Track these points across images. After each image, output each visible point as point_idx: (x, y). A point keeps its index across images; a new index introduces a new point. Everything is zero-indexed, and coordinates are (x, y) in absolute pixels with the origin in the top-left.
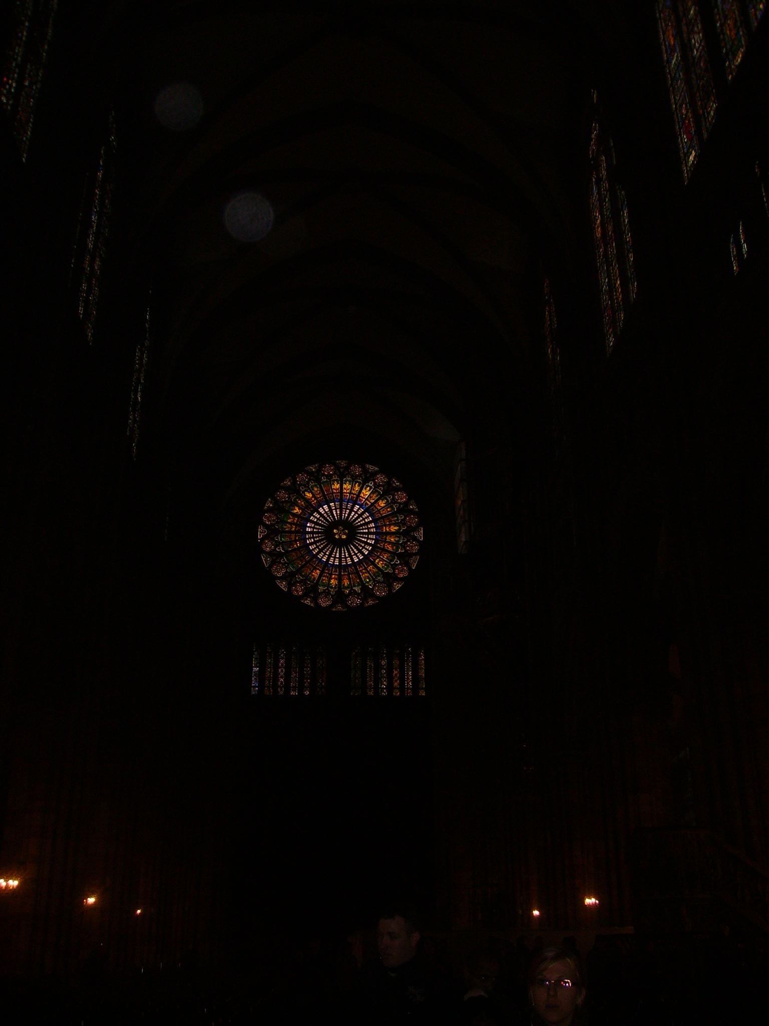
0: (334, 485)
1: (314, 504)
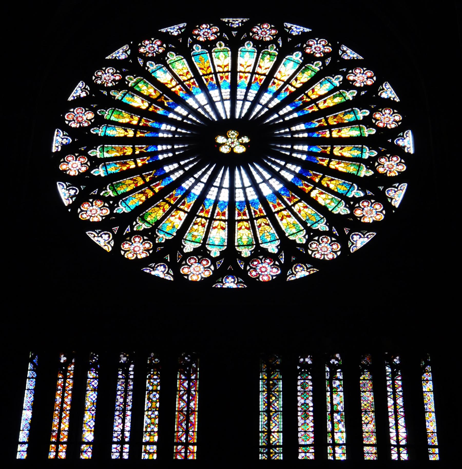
0: (218, 58)
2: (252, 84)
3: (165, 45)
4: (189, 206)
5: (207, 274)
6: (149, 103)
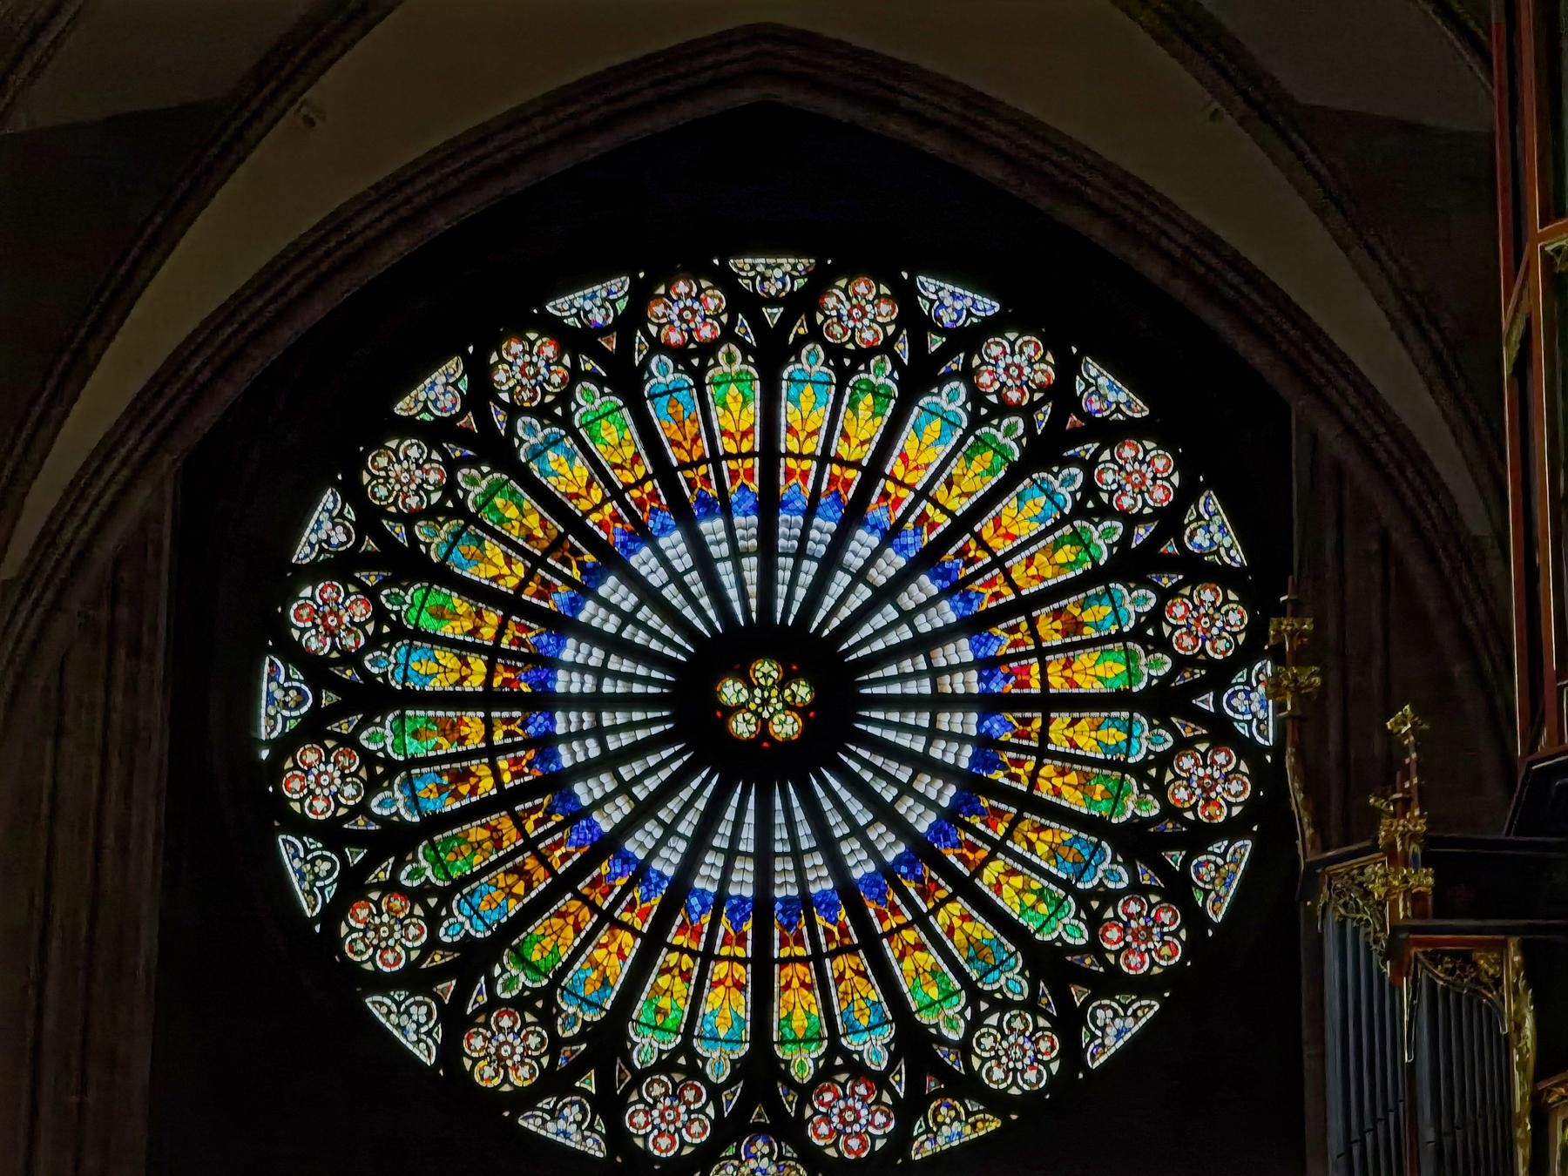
0: (725, 406)
1: (601, 525)
2: (823, 500)
3: (567, 360)
4: (648, 915)
5: (698, 1134)
6: (529, 565)
